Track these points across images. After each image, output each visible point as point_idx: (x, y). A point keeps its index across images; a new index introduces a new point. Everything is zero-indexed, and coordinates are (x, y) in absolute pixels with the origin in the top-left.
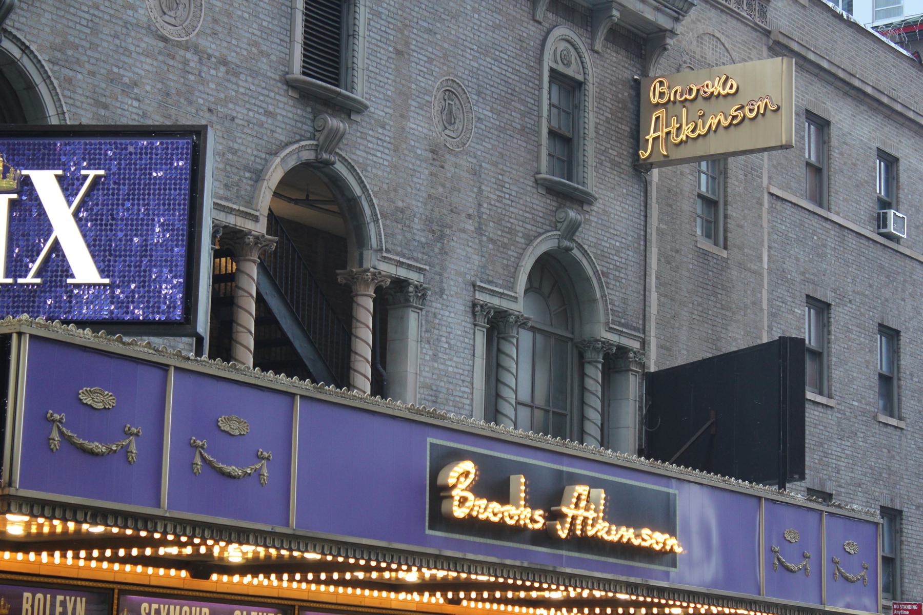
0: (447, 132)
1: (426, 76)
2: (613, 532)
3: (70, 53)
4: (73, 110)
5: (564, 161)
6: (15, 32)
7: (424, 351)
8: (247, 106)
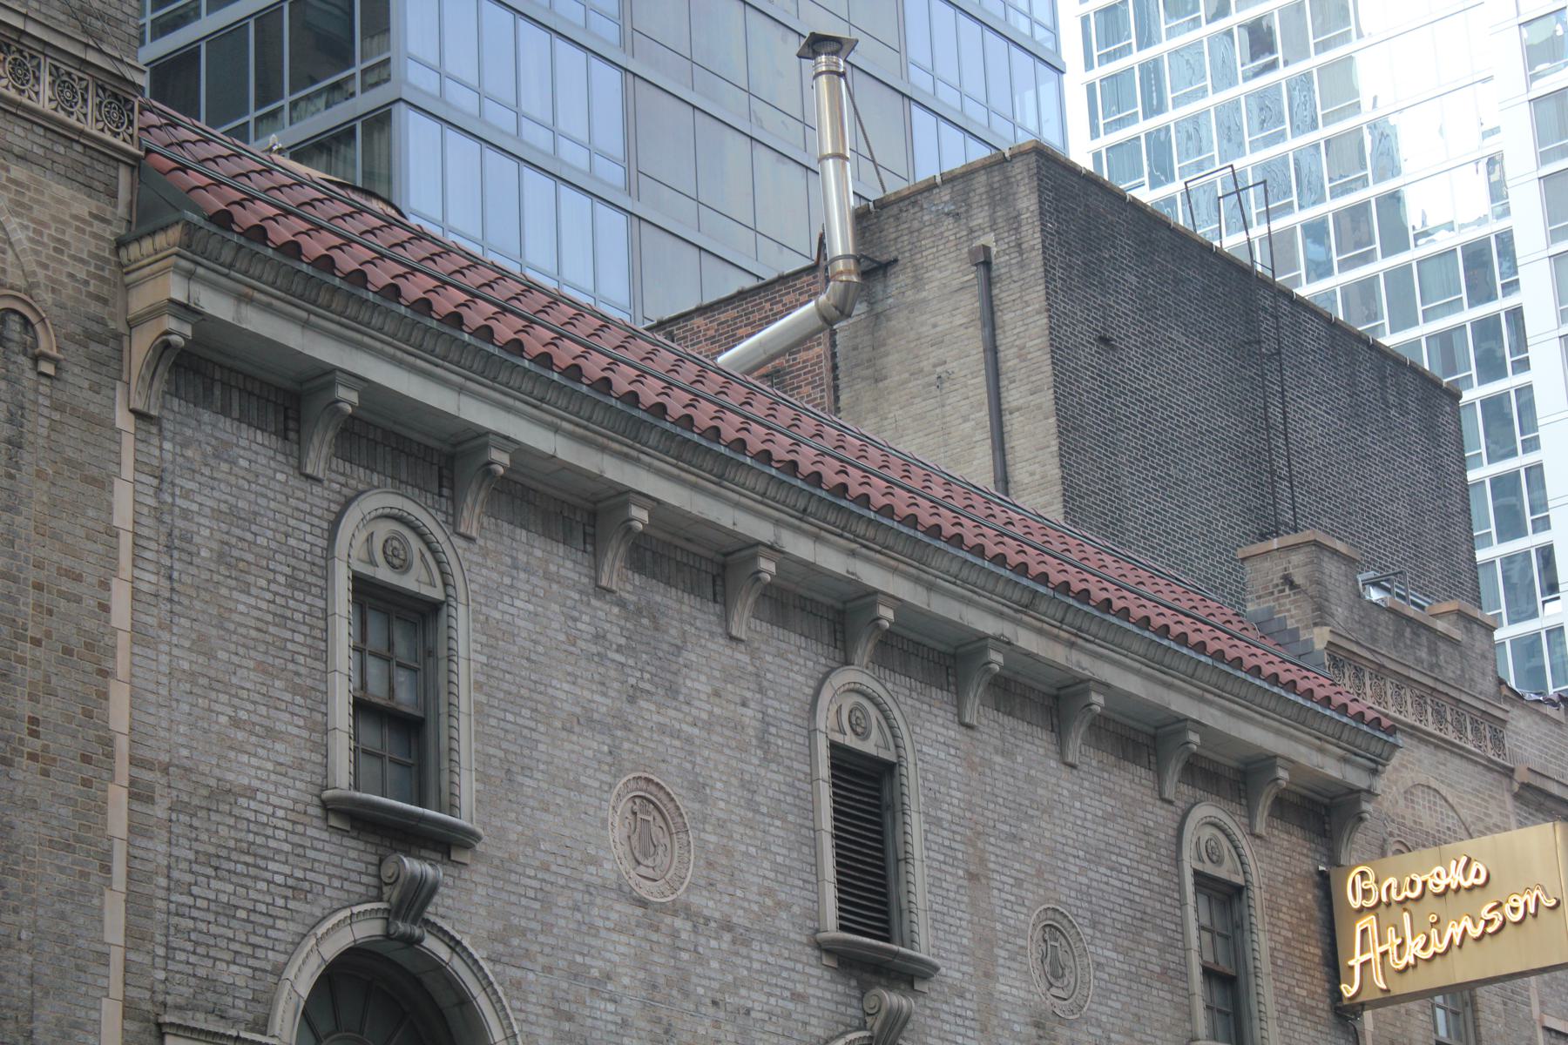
0: (1054, 991)
1: (1016, 908)
3: (515, 942)
4: (526, 1028)
5: (1228, 1015)
6: (440, 922)
8: (767, 989)
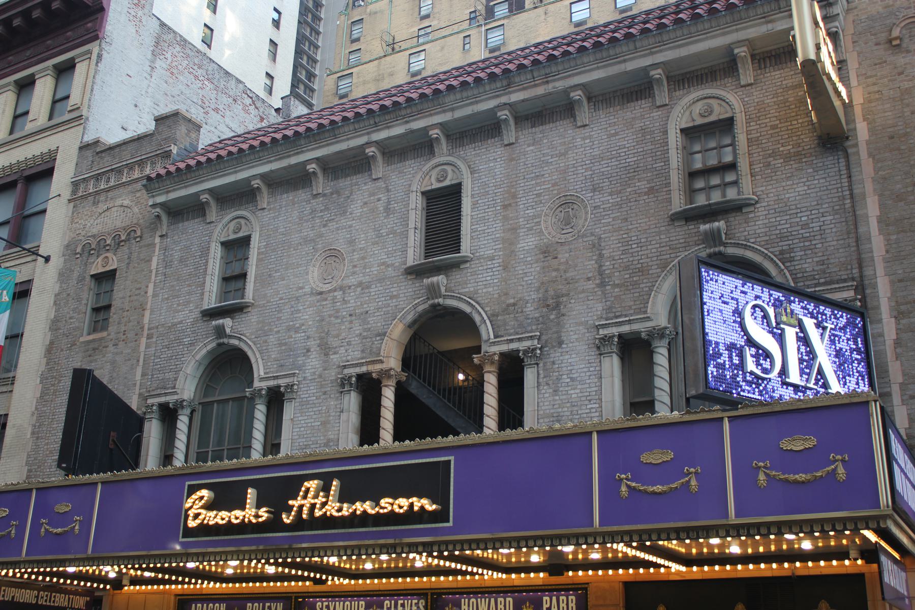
2: (345, 509)
7: (543, 391)
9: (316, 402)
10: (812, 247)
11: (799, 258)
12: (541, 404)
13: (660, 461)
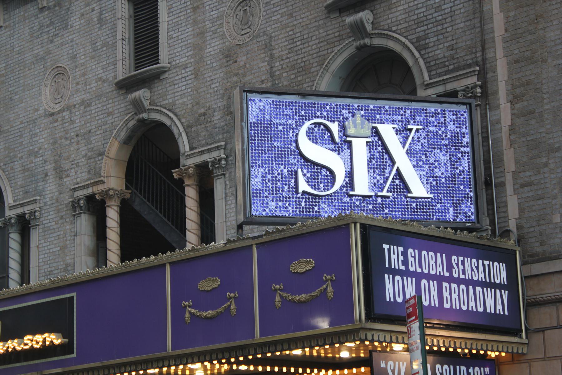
1: (218, 8)
3: (12, 154)
7: (230, 202)
9: (55, 227)
10: (444, 31)
11: (432, 44)
12: (228, 215)
13: (211, 288)
